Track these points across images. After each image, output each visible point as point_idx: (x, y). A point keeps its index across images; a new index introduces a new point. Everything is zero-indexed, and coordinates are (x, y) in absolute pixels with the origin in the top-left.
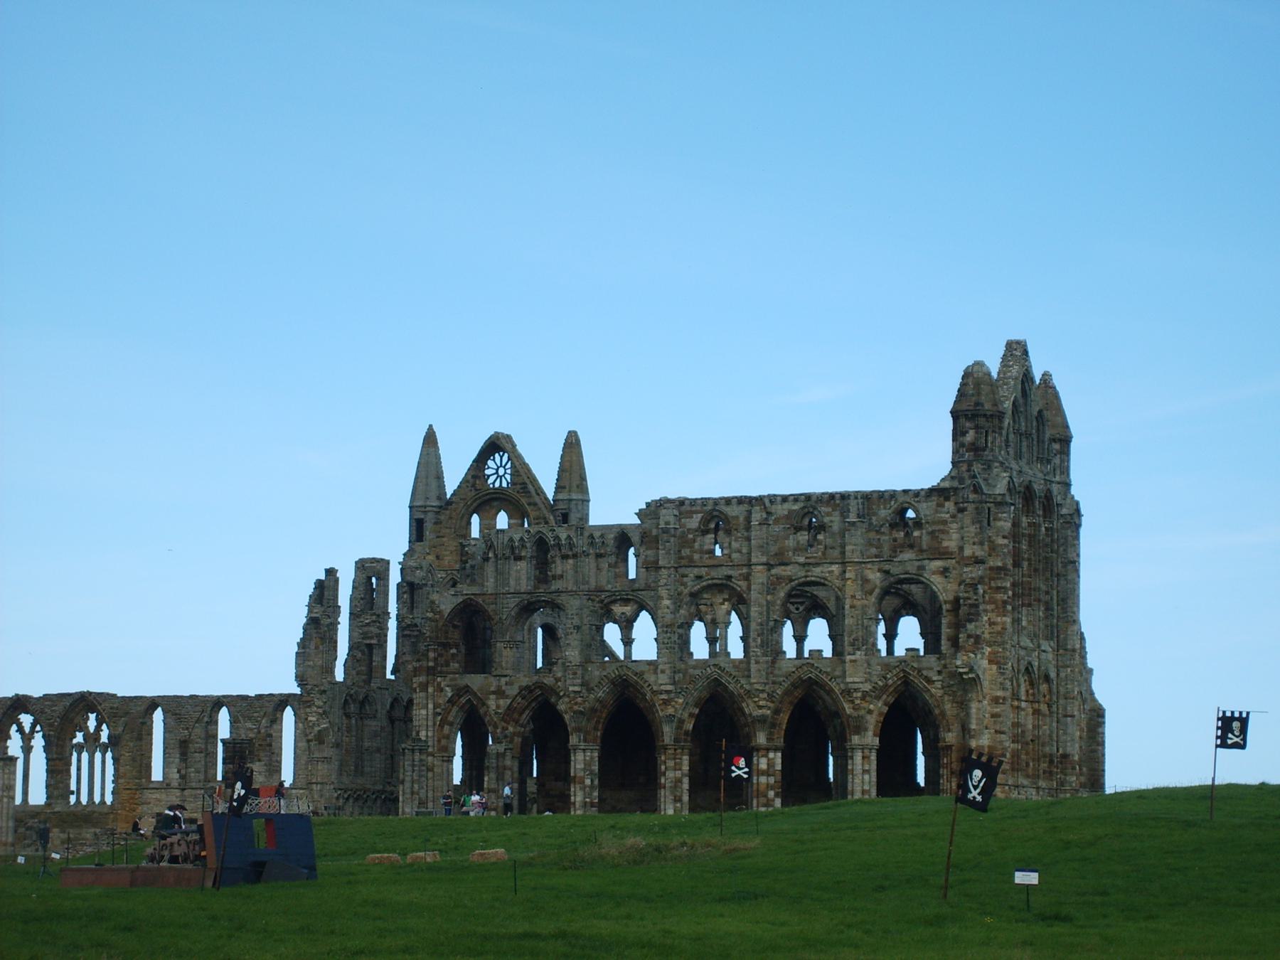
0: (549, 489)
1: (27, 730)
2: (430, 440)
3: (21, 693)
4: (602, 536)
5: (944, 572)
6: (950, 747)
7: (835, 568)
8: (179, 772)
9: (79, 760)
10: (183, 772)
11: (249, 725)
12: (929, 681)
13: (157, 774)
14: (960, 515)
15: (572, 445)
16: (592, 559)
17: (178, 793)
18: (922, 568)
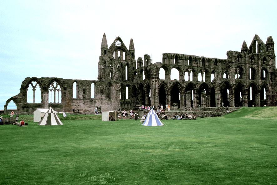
0: (128, 49)
1: (34, 85)
2: (104, 35)
3: (34, 76)
4: (187, 57)
5: (270, 68)
6: (270, 95)
7: (256, 66)
8: (83, 96)
9: (55, 94)
10: (84, 96)
11: (101, 87)
12: (268, 84)
13: (75, 96)
14: (272, 59)
15: (132, 41)
16: (185, 61)
17: (83, 101)
18: (267, 67)
